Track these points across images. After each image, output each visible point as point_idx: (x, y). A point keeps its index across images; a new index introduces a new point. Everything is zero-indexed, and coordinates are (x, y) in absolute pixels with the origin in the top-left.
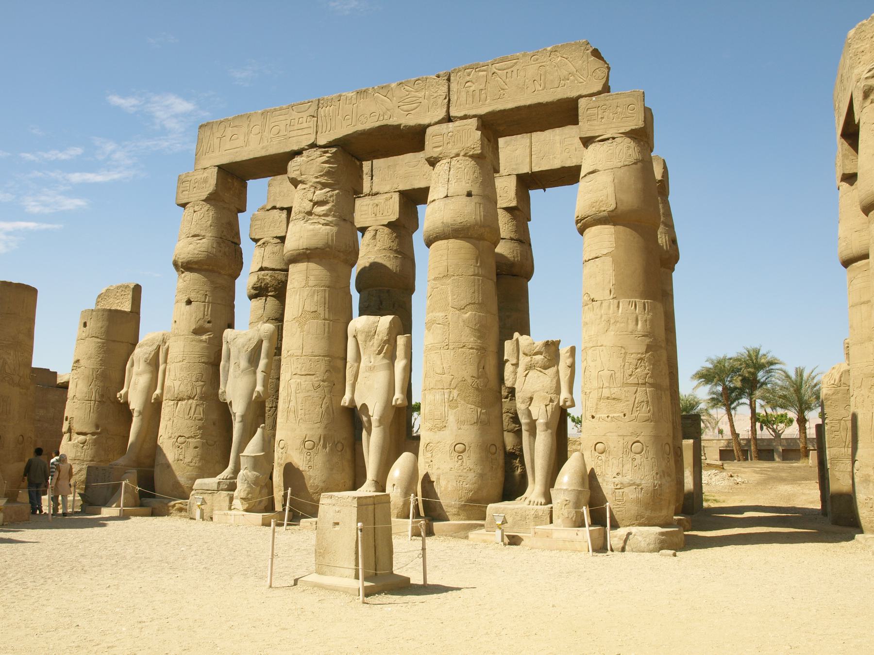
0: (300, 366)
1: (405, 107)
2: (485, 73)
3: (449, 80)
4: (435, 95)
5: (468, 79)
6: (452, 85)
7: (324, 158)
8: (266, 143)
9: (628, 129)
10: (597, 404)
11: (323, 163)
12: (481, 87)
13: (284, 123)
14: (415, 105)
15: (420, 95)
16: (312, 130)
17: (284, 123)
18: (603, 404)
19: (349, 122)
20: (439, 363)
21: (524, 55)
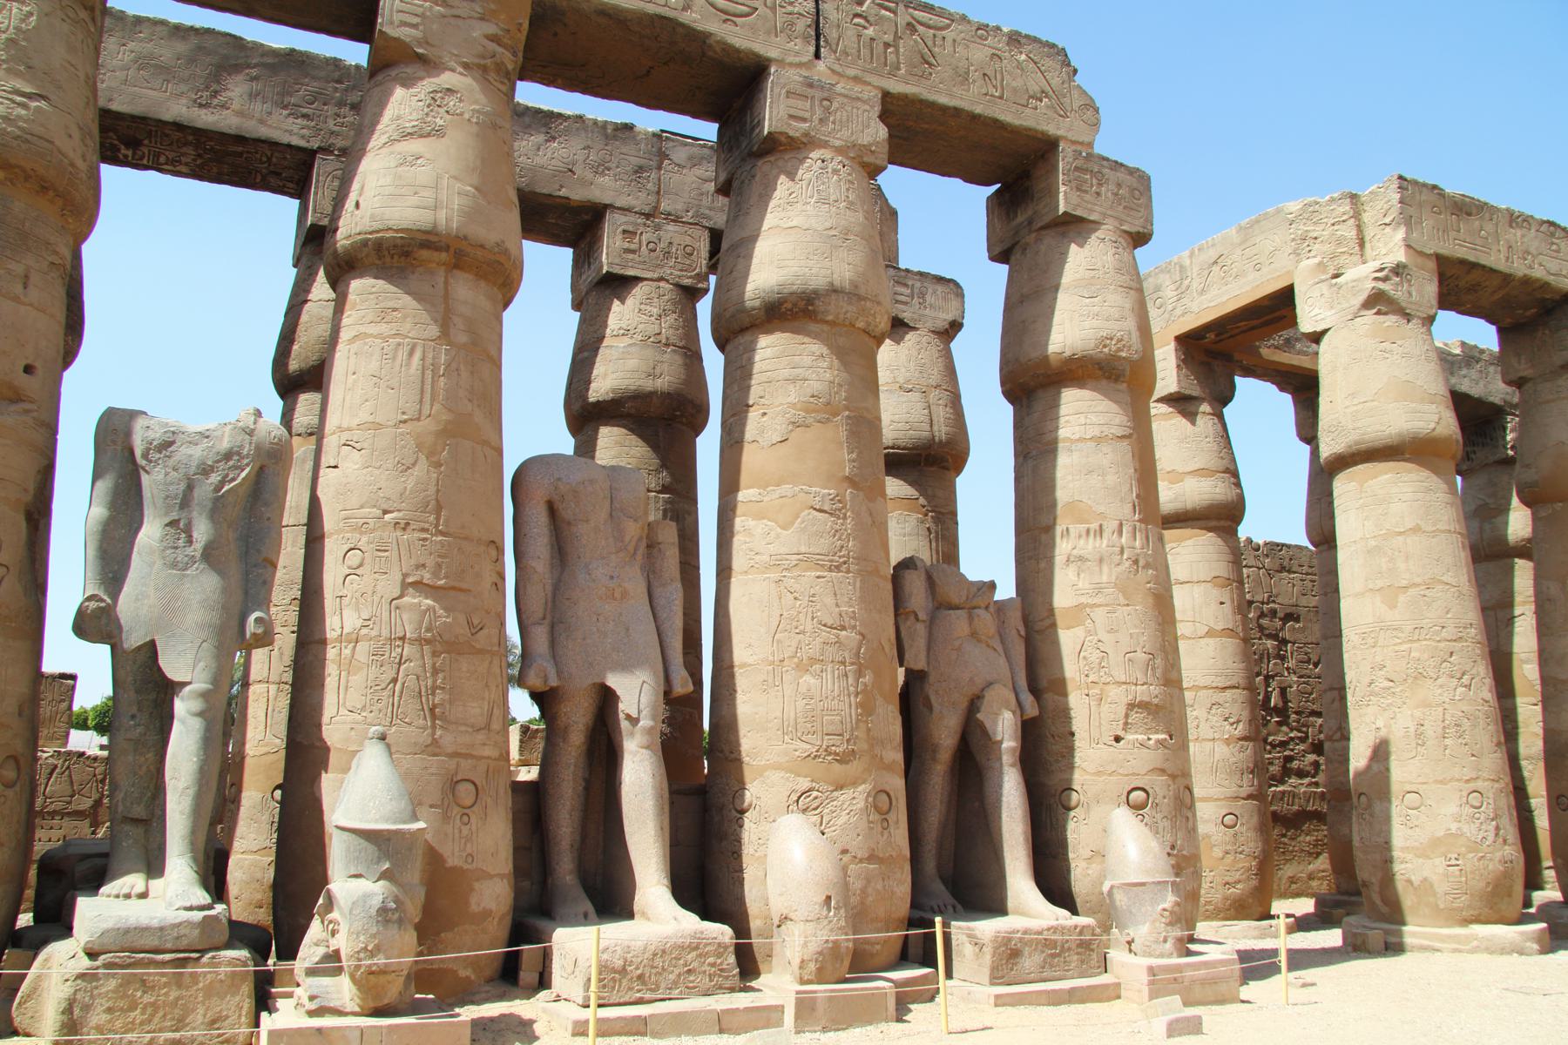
0: (430, 562)
4: (790, 9)
5: (859, 9)
7: (491, 29)
9: (1133, 229)
10: (1127, 716)
11: (488, 37)
12: (889, 38)
18: (1135, 717)
20: (829, 600)
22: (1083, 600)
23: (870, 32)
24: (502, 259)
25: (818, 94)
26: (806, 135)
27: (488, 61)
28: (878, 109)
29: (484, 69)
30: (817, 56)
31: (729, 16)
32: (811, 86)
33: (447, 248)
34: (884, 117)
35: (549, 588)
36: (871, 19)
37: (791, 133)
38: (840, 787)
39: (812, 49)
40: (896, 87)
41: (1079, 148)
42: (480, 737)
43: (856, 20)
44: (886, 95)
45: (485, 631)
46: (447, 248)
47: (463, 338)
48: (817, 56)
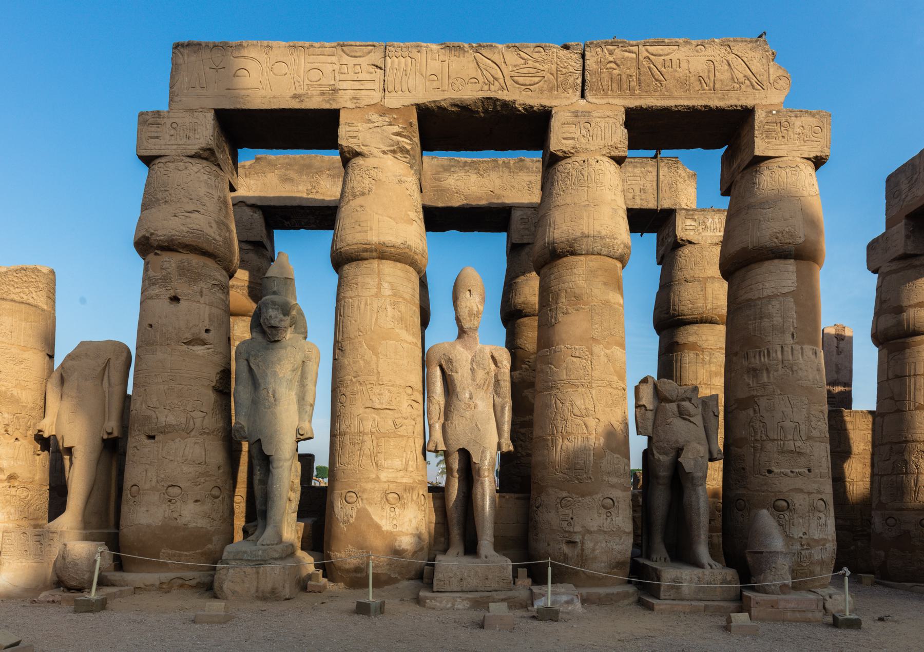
1: (521, 80)
2: (634, 55)
3: (583, 56)
4: (564, 71)
5: (611, 59)
6: (588, 62)
7: (396, 129)
8: (300, 91)
9: (812, 155)
13: (330, 67)
14: (537, 79)
15: (541, 68)
16: (378, 85)
17: (330, 67)
19: (435, 85)
21: (687, 42)
22: (755, 393)
23: (616, 72)
24: (407, 250)
25: (583, 120)
26: (575, 147)
27: (395, 147)
28: (622, 117)
29: (394, 152)
30: (583, 96)
31: (527, 87)
32: (577, 116)
33: (376, 250)
34: (627, 125)
35: (443, 406)
36: (619, 62)
37: (564, 149)
38: (583, 496)
39: (579, 93)
40: (633, 103)
41: (771, 108)
42: (401, 473)
43: (609, 65)
44: (629, 112)
45: (404, 427)
46: (376, 250)
47: (389, 292)
48: (583, 96)
